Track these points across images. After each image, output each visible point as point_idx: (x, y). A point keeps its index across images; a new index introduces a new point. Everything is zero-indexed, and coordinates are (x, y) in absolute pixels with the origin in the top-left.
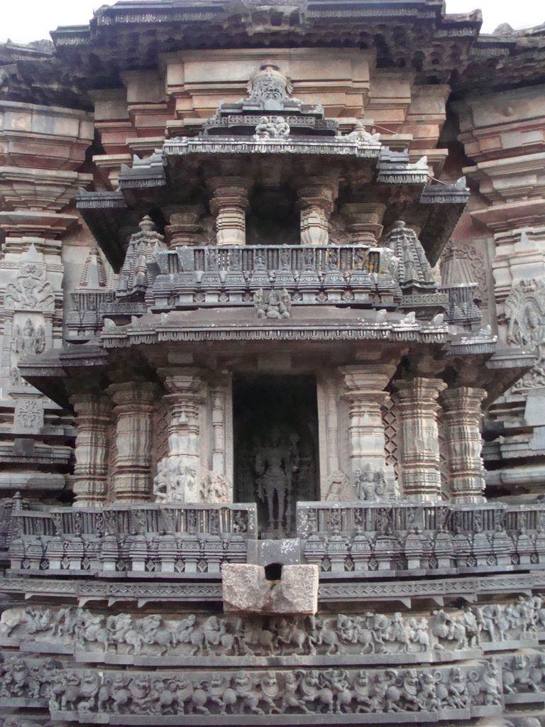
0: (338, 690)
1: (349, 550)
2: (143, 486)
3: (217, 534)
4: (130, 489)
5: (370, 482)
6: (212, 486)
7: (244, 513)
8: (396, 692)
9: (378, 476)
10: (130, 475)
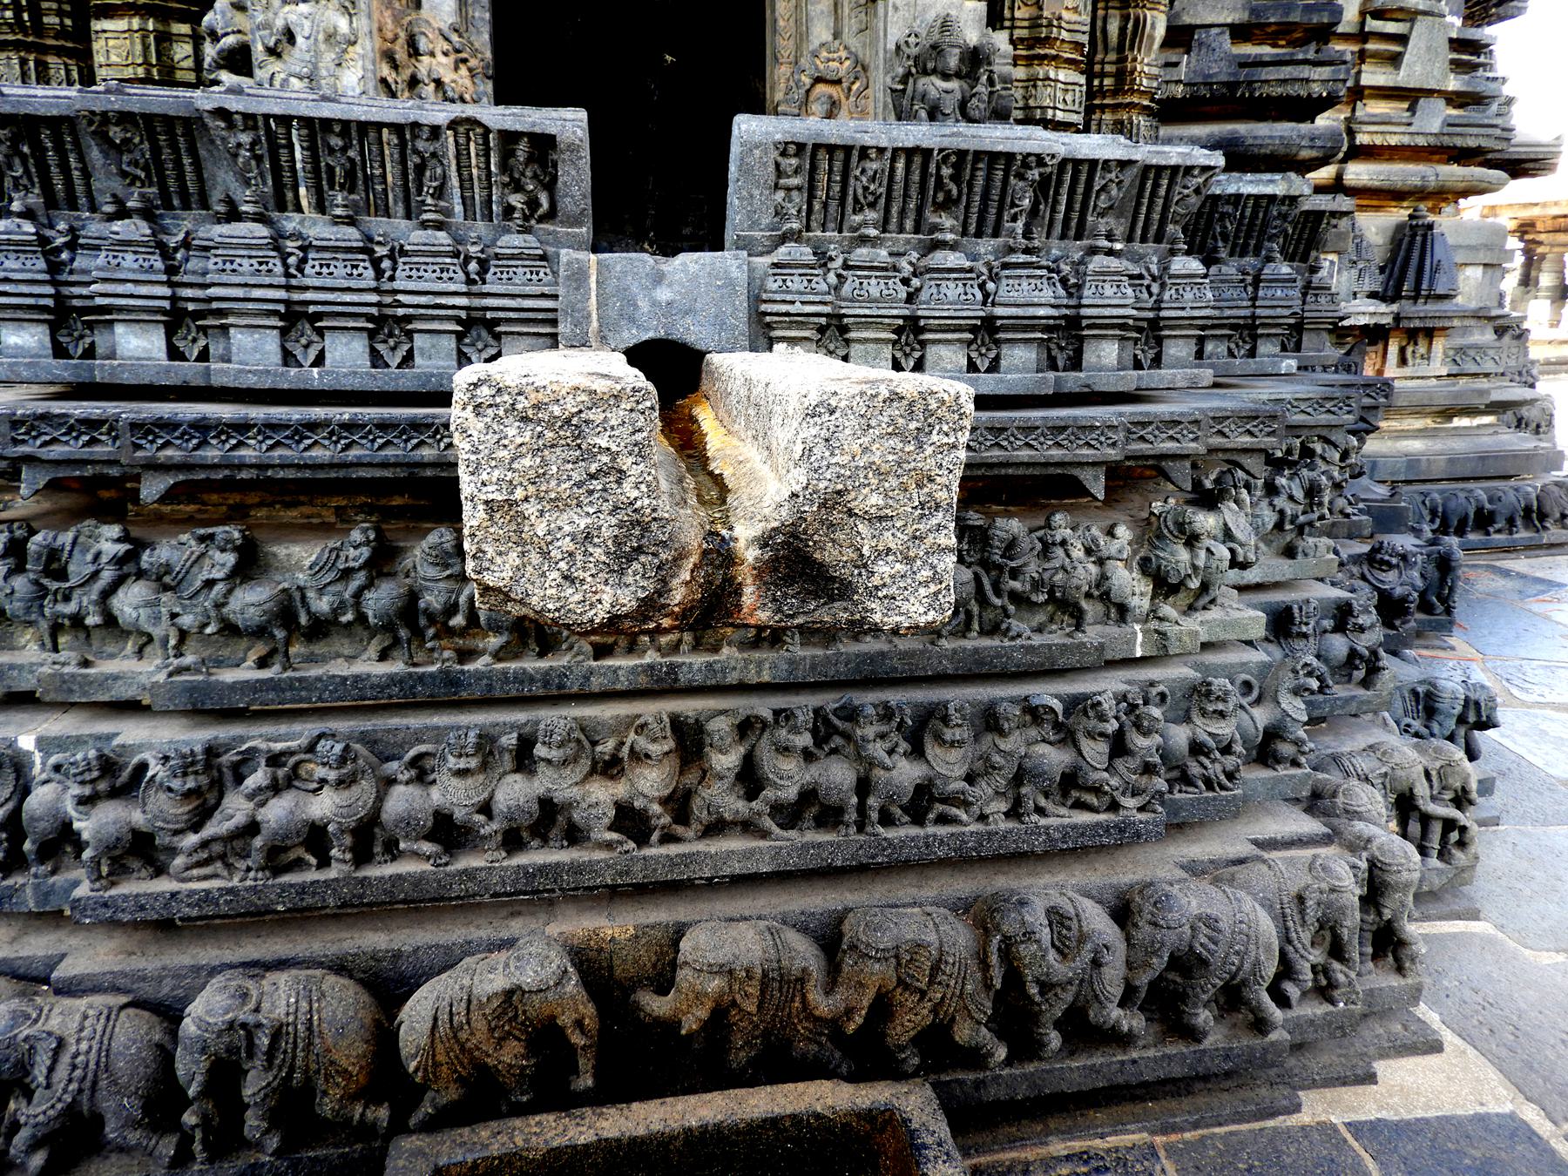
0: (872, 763)
1: (910, 298)
2: (189, 63)
3: (439, 226)
4: (141, 72)
5: (946, 77)
6: (424, 66)
7: (543, 144)
8: (1055, 758)
9: (975, 59)
10: (136, 23)
